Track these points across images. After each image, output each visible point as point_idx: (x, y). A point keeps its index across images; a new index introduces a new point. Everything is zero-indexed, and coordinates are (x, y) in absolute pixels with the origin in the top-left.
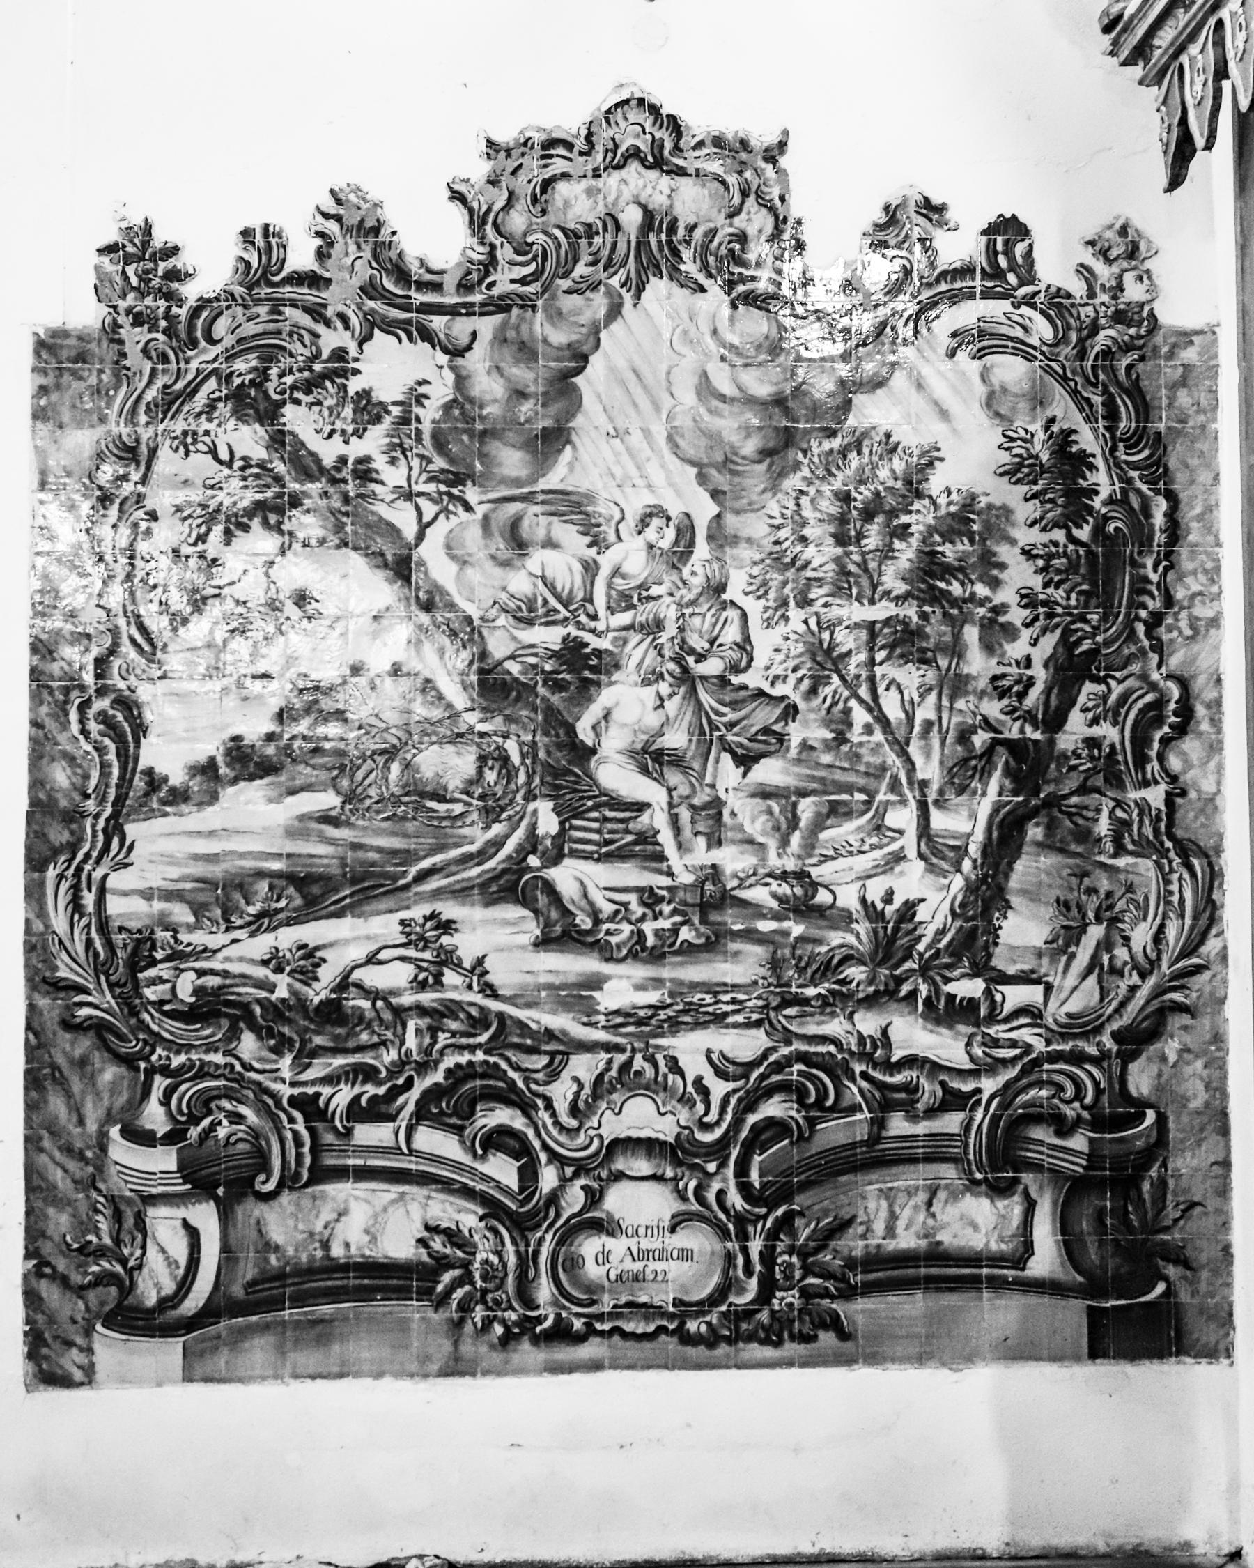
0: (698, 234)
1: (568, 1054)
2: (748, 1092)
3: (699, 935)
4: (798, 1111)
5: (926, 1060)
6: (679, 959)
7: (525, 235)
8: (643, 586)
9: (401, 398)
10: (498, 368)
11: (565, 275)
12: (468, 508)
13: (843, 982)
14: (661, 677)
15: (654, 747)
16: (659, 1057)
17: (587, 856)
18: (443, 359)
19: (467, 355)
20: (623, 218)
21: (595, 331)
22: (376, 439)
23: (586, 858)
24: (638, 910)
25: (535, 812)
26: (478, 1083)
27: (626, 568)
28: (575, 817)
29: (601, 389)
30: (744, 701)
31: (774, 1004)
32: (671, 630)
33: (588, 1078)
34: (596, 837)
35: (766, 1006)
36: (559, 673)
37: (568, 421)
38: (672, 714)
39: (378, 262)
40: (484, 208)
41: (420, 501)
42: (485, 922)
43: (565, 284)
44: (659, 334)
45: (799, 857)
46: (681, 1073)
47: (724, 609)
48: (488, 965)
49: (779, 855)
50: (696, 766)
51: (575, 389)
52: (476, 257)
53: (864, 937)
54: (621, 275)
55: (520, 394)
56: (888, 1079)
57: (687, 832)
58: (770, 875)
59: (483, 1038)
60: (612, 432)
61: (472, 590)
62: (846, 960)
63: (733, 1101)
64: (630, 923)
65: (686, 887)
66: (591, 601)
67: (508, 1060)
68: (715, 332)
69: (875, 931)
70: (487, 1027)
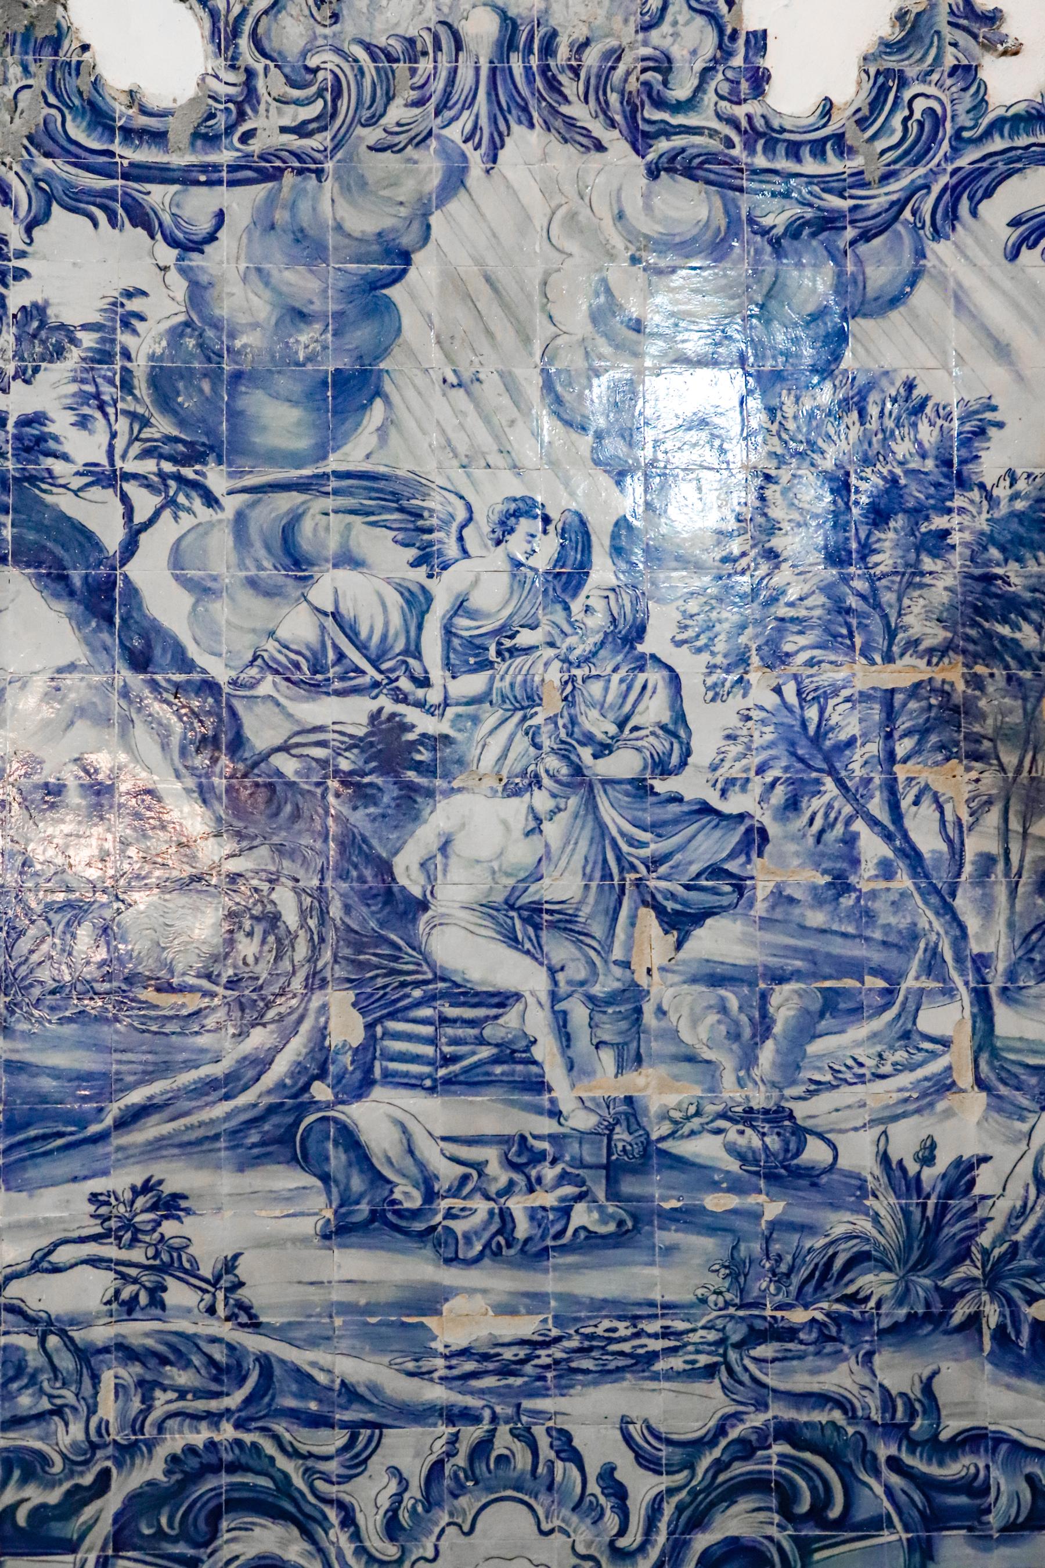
0: (591, 58)
1: (380, 1426)
2: (694, 1493)
3: (605, 1219)
4: (782, 1527)
5: (1000, 1439)
6: (570, 1259)
7: (304, 55)
8: (506, 631)
9: (96, 318)
10: (259, 270)
11: (372, 121)
12: (210, 500)
13: (852, 1300)
14: (536, 781)
15: (525, 900)
16: (539, 1431)
17: (412, 1084)
18: (168, 255)
19: (208, 248)
20: (468, 29)
21: (422, 215)
22: (55, 386)
23: (413, 1086)
24: (499, 1175)
25: (324, 1008)
26: (225, 1479)
27: (477, 601)
28: (392, 1016)
29: (432, 306)
30: (676, 821)
31: (735, 1338)
32: (552, 704)
33: (416, 1472)
34: (428, 1050)
35: (722, 1342)
36: (364, 774)
37: (378, 358)
38: (555, 845)
39: (58, 96)
40: (236, 10)
41: (130, 488)
42: (238, 1196)
43: (373, 135)
44: (529, 218)
45: (774, 1085)
46: (576, 1458)
47: (642, 669)
48: (242, 1271)
49: (740, 1083)
50: (598, 929)
51: (390, 305)
52: (222, 90)
53: (888, 1223)
54: (466, 120)
55: (300, 316)
56: (934, 1470)
57: (582, 1042)
58: (723, 1116)
59: (234, 1400)
60: (452, 379)
61: (216, 634)
62: (857, 1260)
63: (668, 1509)
64: (488, 1198)
65: (582, 1136)
66: (418, 656)
67: (277, 1438)
68: (621, 216)
69: (906, 1213)
70: (242, 1380)
